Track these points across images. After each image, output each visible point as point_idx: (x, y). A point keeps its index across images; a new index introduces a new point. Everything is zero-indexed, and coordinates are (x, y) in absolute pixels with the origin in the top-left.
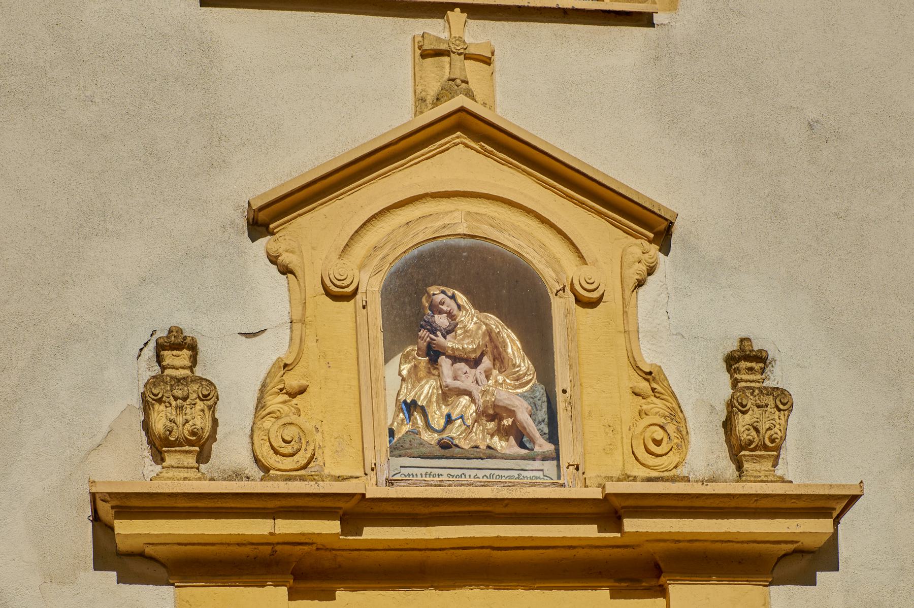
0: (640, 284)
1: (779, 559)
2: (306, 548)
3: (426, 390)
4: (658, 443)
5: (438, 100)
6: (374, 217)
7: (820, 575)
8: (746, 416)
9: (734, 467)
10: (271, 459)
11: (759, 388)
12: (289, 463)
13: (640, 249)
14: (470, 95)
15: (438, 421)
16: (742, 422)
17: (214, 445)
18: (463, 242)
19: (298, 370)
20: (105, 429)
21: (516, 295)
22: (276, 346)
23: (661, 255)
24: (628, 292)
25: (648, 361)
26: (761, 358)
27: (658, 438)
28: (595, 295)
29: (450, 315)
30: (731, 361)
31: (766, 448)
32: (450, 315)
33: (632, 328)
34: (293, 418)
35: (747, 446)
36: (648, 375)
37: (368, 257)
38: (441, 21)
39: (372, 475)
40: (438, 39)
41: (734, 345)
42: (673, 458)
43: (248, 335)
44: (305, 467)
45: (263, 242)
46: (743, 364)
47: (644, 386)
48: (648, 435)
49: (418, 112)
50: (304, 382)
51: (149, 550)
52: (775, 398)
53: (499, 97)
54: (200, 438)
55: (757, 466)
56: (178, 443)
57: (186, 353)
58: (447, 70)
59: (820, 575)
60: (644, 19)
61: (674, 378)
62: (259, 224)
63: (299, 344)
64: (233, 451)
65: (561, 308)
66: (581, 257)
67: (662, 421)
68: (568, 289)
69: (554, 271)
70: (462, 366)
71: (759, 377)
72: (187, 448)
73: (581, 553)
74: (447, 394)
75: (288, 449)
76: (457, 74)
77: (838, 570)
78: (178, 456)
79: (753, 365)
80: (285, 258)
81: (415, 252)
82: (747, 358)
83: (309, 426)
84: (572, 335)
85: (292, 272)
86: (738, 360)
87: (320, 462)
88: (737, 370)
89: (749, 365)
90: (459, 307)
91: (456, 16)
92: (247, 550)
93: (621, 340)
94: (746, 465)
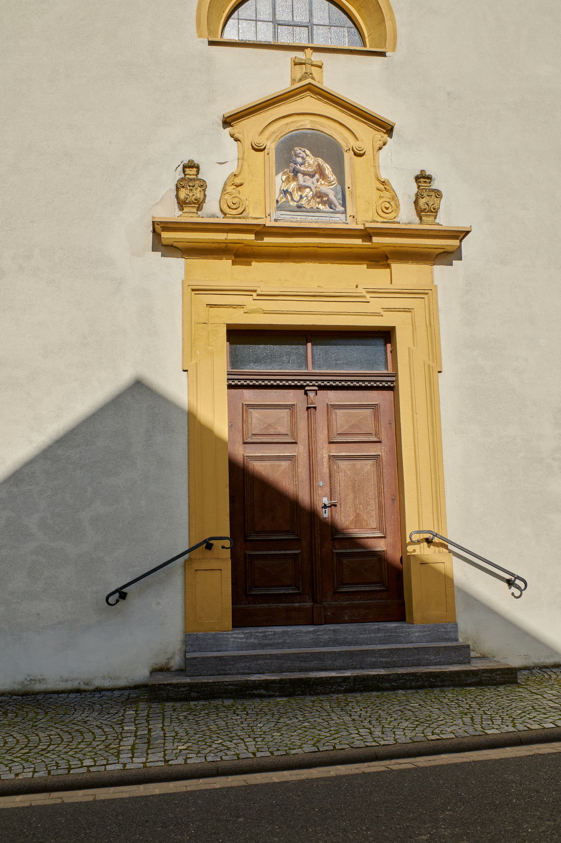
0: (380, 148)
1: (437, 255)
2: (240, 245)
4: (387, 208)
5: (300, 80)
6: (274, 121)
7: (454, 262)
8: (424, 199)
10: (227, 210)
12: (234, 212)
13: (380, 136)
14: (313, 78)
16: (422, 202)
17: (204, 204)
19: (240, 177)
20: (160, 198)
21: (331, 152)
22: (231, 168)
23: (389, 138)
24: (375, 152)
25: (383, 177)
26: (429, 178)
27: (387, 207)
28: (362, 152)
29: (303, 158)
30: (417, 178)
31: (432, 212)
32: (303, 158)
33: (377, 165)
34: (237, 195)
35: (424, 211)
36: (383, 183)
37: (270, 136)
38: (303, 53)
39: (269, 217)
40: (301, 59)
41: (419, 173)
43: (220, 163)
44: (241, 214)
45: (229, 129)
46: (422, 180)
47: (381, 187)
50: (242, 182)
52: (435, 193)
53: (324, 80)
54: (198, 202)
55: (428, 219)
57: (195, 170)
59: (454, 262)
60: (383, 54)
61: (394, 184)
62: (227, 122)
63: (241, 168)
65: (348, 157)
66: (356, 138)
67: (389, 200)
68: (351, 149)
69: (345, 143)
70: (307, 177)
71: (428, 185)
72: (193, 205)
73: (355, 250)
74: (301, 188)
75: (235, 207)
76: (308, 71)
77: (461, 260)
78: (189, 208)
79: (426, 180)
80: (237, 135)
81: (289, 134)
82: (424, 177)
83: (243, 198)
84: (352, 167)
85: (239, 141)
86: (420, 178)
88: (420, 182)
89: (424, 180)
90: (307, 155)
91: (308, 51)
92: (216, 245)
93: (372, 169)
94: (423, 218)
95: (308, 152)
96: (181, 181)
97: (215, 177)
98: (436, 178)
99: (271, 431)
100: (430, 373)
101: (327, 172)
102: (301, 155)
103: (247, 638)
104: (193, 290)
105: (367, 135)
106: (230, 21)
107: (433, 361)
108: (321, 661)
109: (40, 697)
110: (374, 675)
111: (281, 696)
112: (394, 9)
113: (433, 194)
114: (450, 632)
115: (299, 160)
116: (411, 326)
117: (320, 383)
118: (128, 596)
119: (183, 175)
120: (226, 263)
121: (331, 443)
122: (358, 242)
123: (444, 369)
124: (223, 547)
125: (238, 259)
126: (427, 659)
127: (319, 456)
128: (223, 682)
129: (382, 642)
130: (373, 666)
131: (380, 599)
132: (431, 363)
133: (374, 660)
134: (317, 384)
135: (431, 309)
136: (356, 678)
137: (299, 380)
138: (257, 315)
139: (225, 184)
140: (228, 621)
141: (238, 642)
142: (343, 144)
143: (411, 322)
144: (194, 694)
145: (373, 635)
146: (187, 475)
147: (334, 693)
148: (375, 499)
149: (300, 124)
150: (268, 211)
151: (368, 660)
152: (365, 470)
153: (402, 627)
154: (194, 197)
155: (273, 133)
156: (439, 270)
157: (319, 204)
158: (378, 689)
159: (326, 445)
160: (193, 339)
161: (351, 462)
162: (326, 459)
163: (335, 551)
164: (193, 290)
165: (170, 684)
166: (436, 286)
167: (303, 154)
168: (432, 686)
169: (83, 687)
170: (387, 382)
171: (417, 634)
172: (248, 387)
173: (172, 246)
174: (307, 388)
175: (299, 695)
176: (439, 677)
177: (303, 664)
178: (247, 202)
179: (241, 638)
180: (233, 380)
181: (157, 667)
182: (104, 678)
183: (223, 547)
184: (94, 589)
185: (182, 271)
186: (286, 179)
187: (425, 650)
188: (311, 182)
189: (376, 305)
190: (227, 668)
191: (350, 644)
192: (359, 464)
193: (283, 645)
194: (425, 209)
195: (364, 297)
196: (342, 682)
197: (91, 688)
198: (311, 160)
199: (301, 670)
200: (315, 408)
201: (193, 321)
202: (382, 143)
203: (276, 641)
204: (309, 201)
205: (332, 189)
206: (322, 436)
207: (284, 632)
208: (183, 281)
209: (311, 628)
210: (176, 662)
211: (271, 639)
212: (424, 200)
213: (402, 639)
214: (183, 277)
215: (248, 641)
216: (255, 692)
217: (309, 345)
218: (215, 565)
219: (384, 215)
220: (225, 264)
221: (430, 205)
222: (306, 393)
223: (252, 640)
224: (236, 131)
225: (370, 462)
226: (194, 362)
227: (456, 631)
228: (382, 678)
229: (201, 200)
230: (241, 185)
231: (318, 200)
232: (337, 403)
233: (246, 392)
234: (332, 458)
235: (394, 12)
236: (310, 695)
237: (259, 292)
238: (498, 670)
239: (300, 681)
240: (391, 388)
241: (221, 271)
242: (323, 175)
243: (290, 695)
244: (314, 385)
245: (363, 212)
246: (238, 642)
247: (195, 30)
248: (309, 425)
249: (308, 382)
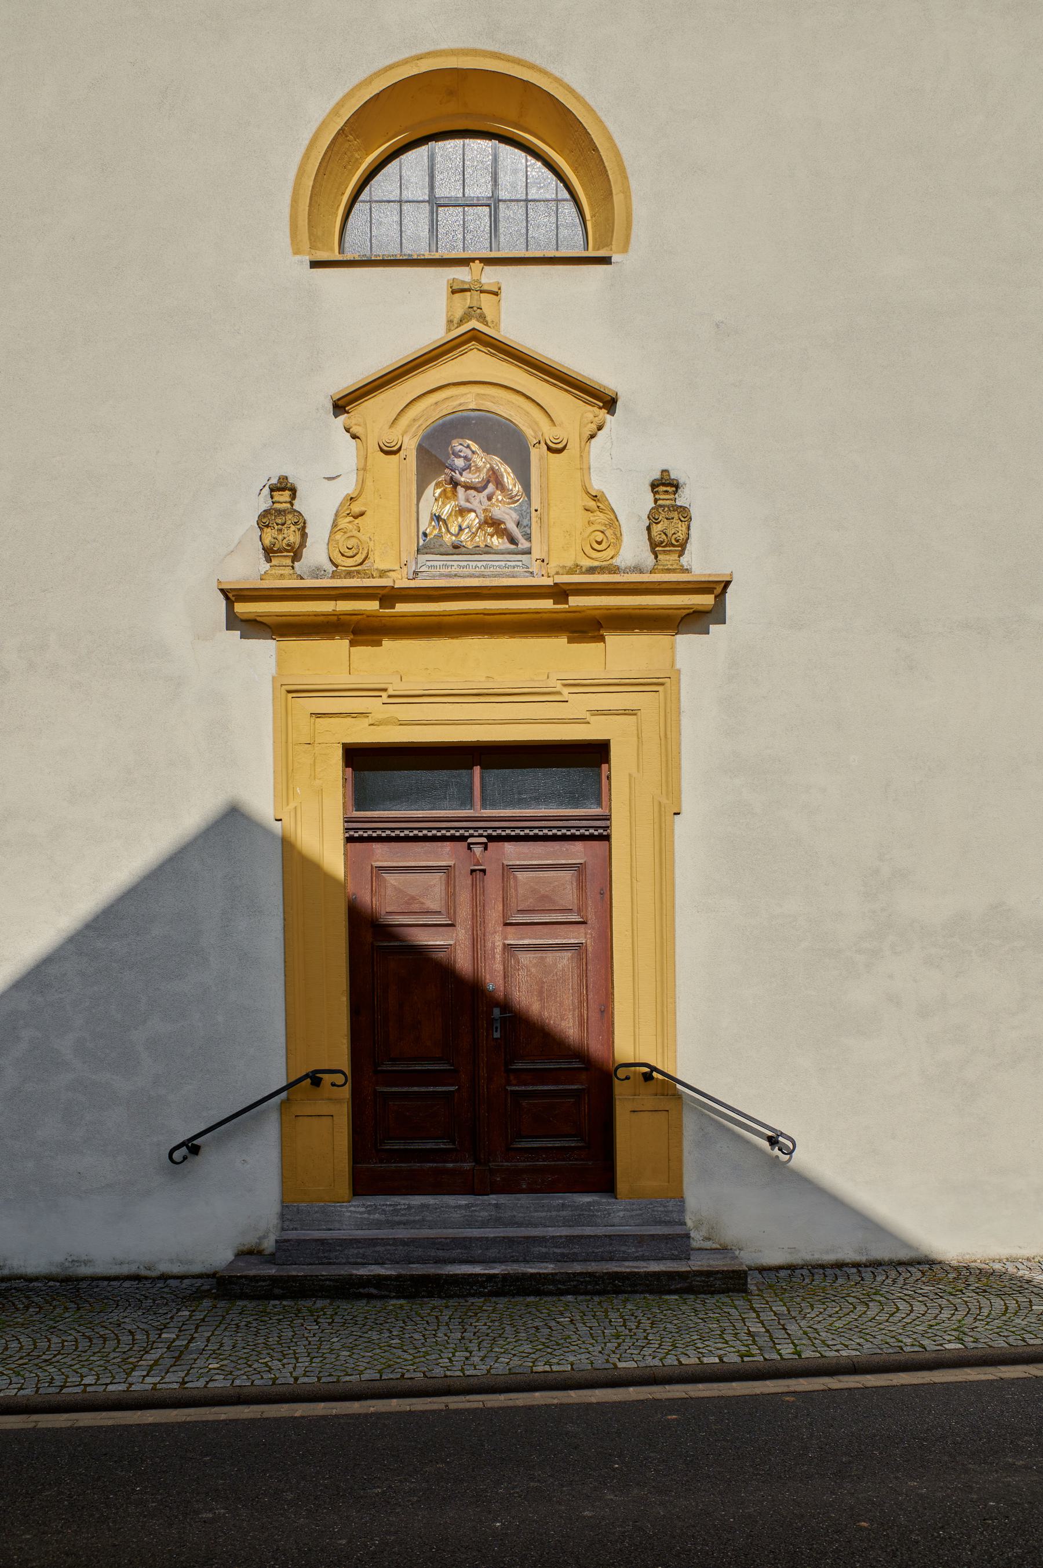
0: (592, 437)
1: (682, 618)
3: (446, 511)
4: (599, 543)
5: (461, 322)
8: (659, 526)
9: (653, 556)
10: (339, 560)
11: (668, 507)
12: (350, 562)
13: (593, 413)
14: (482, 318)
15: (454, 529)
16: (656, 529)
18: (472, 414)
19: (361, 500)
20: (236, 542)
22: (347, 486)
23: (608, 417)
24: (583, 443)
27: (599, 540)
28: (560, 446)
30: (654, 486)
31: (674, 546)
33: (585, 466)
34: (355, 533)
36: (595, 498)
37: (409, 426)
38: (467, 268)
40: (463, 282)
41: (657, 475)
42: (610, 552)
43: (329, 479)
44: (361, 564)
45: (343, 418)
46: (662, 488)
47: (592, 504)
48: (592, 537)
49: (449, 330)
50: (363, 509)
51: (258, 619)
53: (503, 316)
54: (293, 548)
55: (668, 557)
56: (279, 551)
57: (287, 493)
58: (469, 301)
60: (606, 261)
62: (340, 406)
63: (362, 484)
64: (316, 553)
65: (536, 455)
66: (552, 420)
67: (602, 528)
68: (542, 443)
71: (672, 496)
73: (545, 616)
74: (462, 512)
75: (350, 553)
76: (475, 304)
79: (668, 489)
80: (355, 430)
81: (441, 421)
82: (664, 485)
83: (364, 538)
84: (544, 474)
86: (658, 486)
87: (371, 560)
89: (665, 489)
91: (477, 266)
92: (322, 618)
93: (578, 474)
95: (475, 447)
97: (318, 506)
98: (687, 482)
99: (416, 907)
100: (660, 815)
102: (462, 454)
103: (369, 1213)
104: (289, 692)
105: (570, 413)
107: (667, 795)
108: (465, 1249)
109: (84, 1285)
110: (532, 1274)
111: (398, 1298)
112: (629, 171)
113: (675, 515)
114: (672, 1212)
115: (460, 463)
116: (635, 739)
117: (490, 831)
118: (202, 1150)
119: (270, 501)
120: (340, 645)
121: (506, 924)
122: (547, 604)
123: (685, 808)
124: (333, 1085)
125: (359, 638)
126: (624, 1252)
127: (489, 944)
128: (317, 1276)
129: (567, 1223)
130: (543, 1258)
131: (576, 1160)
132: (664, 801)
133: (544, 1250)
134: (485, 834)
135: (668, 710)
136: (505, 1277)
137: (457, 829)
138: (389, 727)
139: (336, 515)
140: (344, 1187)
141: (355, 1217)
142: (529, 433)
143: (635, 732)
144: (277, 1291)
145: (554, 1213)
146: (282, 977)
147: (473, 1295)
148: (574, 1010)
149: (458, 402)
150: (404, 560)
151: (537, 1250)
152: (560, 966)
153: (599, 1203)
155: (414, 420)
156: (685, 643)
157: (492, 536)
158: (539, 1293)
159: (500, 928)
160: (290, 771)
161: (539, 954)
162: (499, 950)
163: (509, 1088)
164: (289, 692)
165: (246, 1277)
166: (679, 671)
168: (617, 1292)
169: (144, 1272)
170: (596, 828)
171: (621, 1214)
172: (379, 839)
173: (255, 621)
174: (470, 840)
175: (423, 1297)
176: (628, 1279)
177: (440, 1253)
178: (371, 544)
179: (361, 1213)
180: (356, 830)
181: (245, 1248)
182: (171, 1261)
183: (333, 1085)
184: (155, 1140)
185: (273, 661)
187: (623, 1238)
189: (579, 704)
190: (333, 1255)
191: (520, 1225)
192: (550, 957)
193: (421, 1224)
194: (662, 542)
195: (559, 693)
196: (486, 1281)
197: (154, 1274)
198: (480, 460)
199: (438, 1261)
200: (484, 871)
201: (290, 741)
202: (594, 427)
203: (412, 1218)
204: (474, 534)
205: (514, 509)
206: (494, 915)
207: (423, 1206)
208: (273, 677)
209: (463, 1200)
210: (269, 1245)
211: (403, 1215)
212: (660, 527)
213: (599, 1220)
214: (274, 671)
215: (372, 1217)
216: (361, 1290)
217: (477, 770)
218: (324, 1108)
219: (594, 554)
220: (337, 648)
221: (670, 535)
222: (469, 848)
223: (377, 1216)
224: (354, 422)
225: (569, 954)
226: (292, 805)
227: (682, 1210)
228: (545, 1278)
229: (297, 546)
230: (362, 514)
231: (490, 530)
232: (518, 863)
233: (377, 847)
234: (507, 948)
235: (629, 176)
236: (440, 1297)
237: (391, 692)
238: (718, 1272)
239: (425, 1279)
240: (607, 838)
241: (330, 659)
243: (410, 1297)
244: (481, 836)
245: (556, 553)
246: (355, 1217)
248: (474, 898)
249: (471, 831)
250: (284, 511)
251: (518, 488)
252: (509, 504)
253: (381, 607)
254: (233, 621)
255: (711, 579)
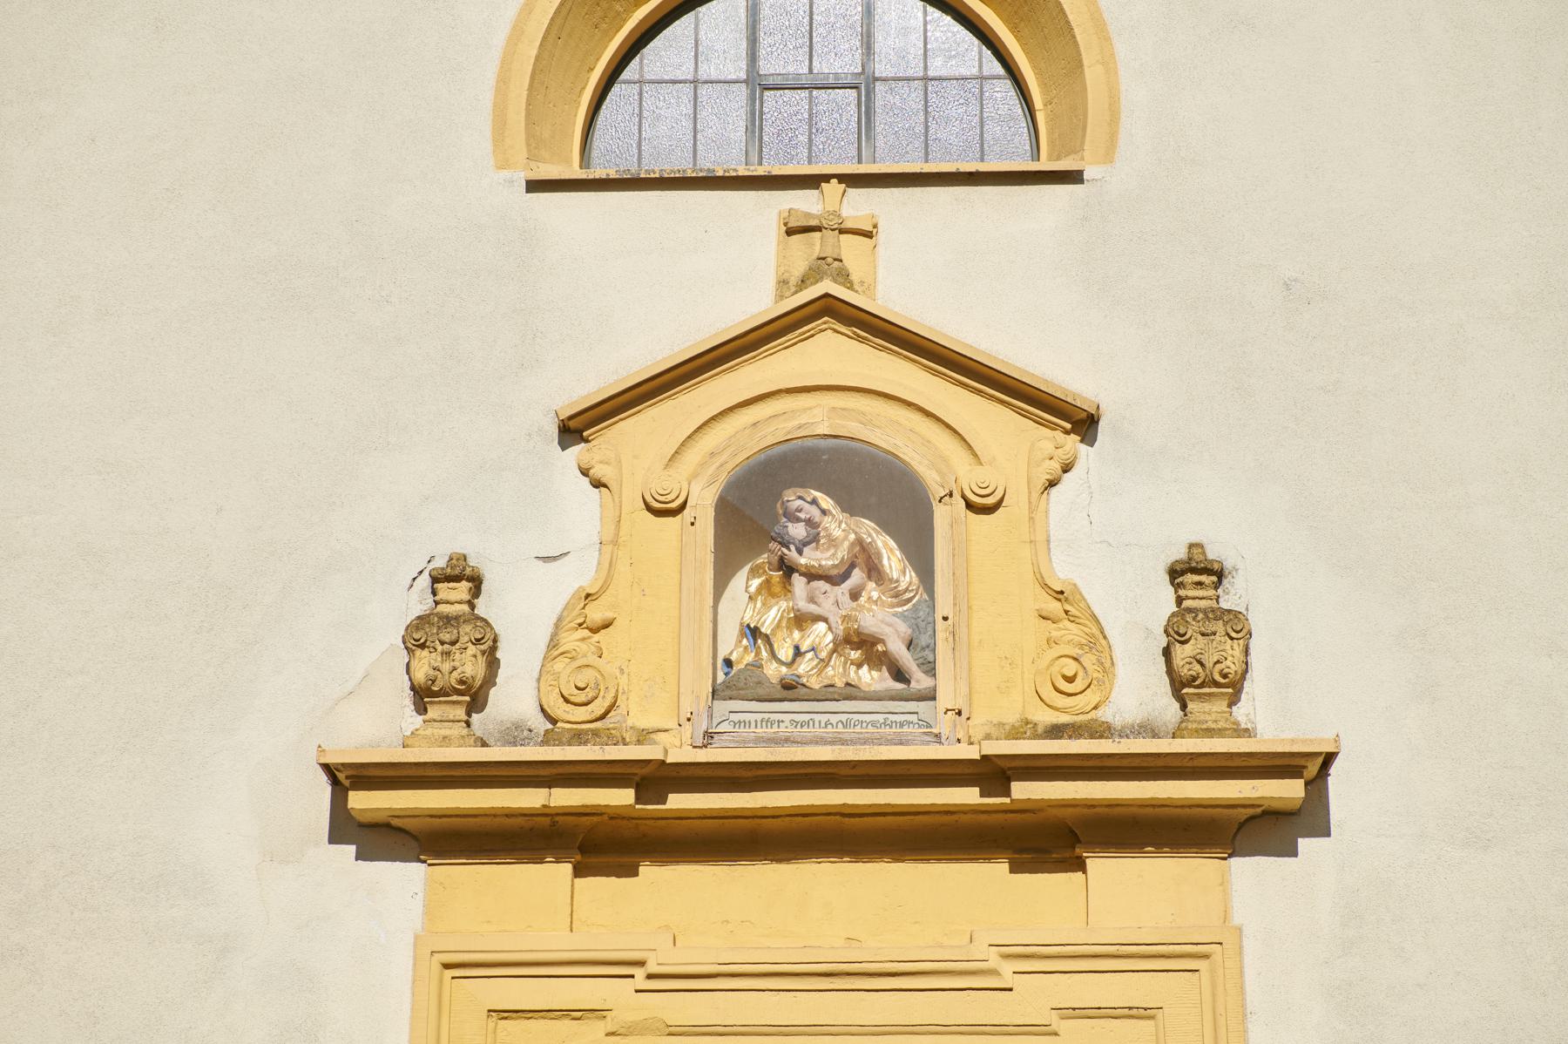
0: (1052, 484)
1: (1242, 825)
2: (595, 819)
3: (770, 618)
5: (803, 283)
6: (713, 419)
7: (1303, 843)
9: (1177, 705)
12: (581, 714)
13: (1054, 441)
14: (843, 277)
15: (785, 653)
17: (493, 691)
18: (823, 443)
22: (579, 573)
23: (1083, 448)
24: (1035, 495)
25: (1061, 576)
27: (1070, 674)
30: (1175, 573)
31: (1217, 684)
33: (1040, 537)
34: (592, 659)
35: (1191, 681)
37: (703, 465)
38: (815, 192)
39: (688, 726)
41: (1180, 553)
42: (1091, 697)
43: (547, 559)
45: (576, 450)
46: (1190, 578)
47: (1054, 607)
48: (1055, 669)
49: (780, 297)
50: (609, 615)
51: (395, 822)
53: (881, 273)
54: (470, 687)
55: (1207, 706)
56: (443, 692)
57: (465, 585)
58: (817, 248)
59: (1303, 843)
60: (1074, 177)
61: (1096, 597)
62: (572, 431)
64: (515, 697)
65: (946, 517)
66: (975, 455)
67: (1076, 652)
68: (957, 495)
69: (939, 472)
71: (1211, 592)
72: (455, 698)
73: (964, 818)
75: (582, 697)
76: (829, 252)
78: (444, 707)
79: (1203, 578)
80: (598, 471)
82: (1194, 571)
83: (608, 666)
85: (605, 486)
86: (1183, 573)
87: (622, 710)
88: (1180, 586)
89: (1197, 578)
91: (833, 187)
92: (520, 820)
94: (1191, 706)
95: (826, 502)
96: (417, 629)
98: (1240, 565)
101: (885, 562)
102: (802, 515)
104: (447, 966)
105: (1008, 442)
106: (616, 89)
115: (798, 531)
119: (430, 600)
125: (593, 860)
139: (557, 625)
149: (796, 423)
154: (455, 674)
156: (1249, 873)
164: (447, 966)
166: (1240, 929)
167: (814, 512)
173: (388, 826)
178: (623, 681)
185: (417, 906)
186: (759, 590)
188: (832, 600)
194: (1194, 679)
202: (1056, 466)
204: (825, 663)
208: (416, 937)
212: (1189, 649)
219: (1061, 701)
224: (597, 458)
229: (478, 683)
231: (855, 655)
237: (653, 968)
242: (874, 571)
245: (986, 698)
247: (488, 145)
250: (457, 618)
251: (909, 578)
252: (893, 606)
253: (638, 800)
254: (343, 827)
255: (1295, 749)
